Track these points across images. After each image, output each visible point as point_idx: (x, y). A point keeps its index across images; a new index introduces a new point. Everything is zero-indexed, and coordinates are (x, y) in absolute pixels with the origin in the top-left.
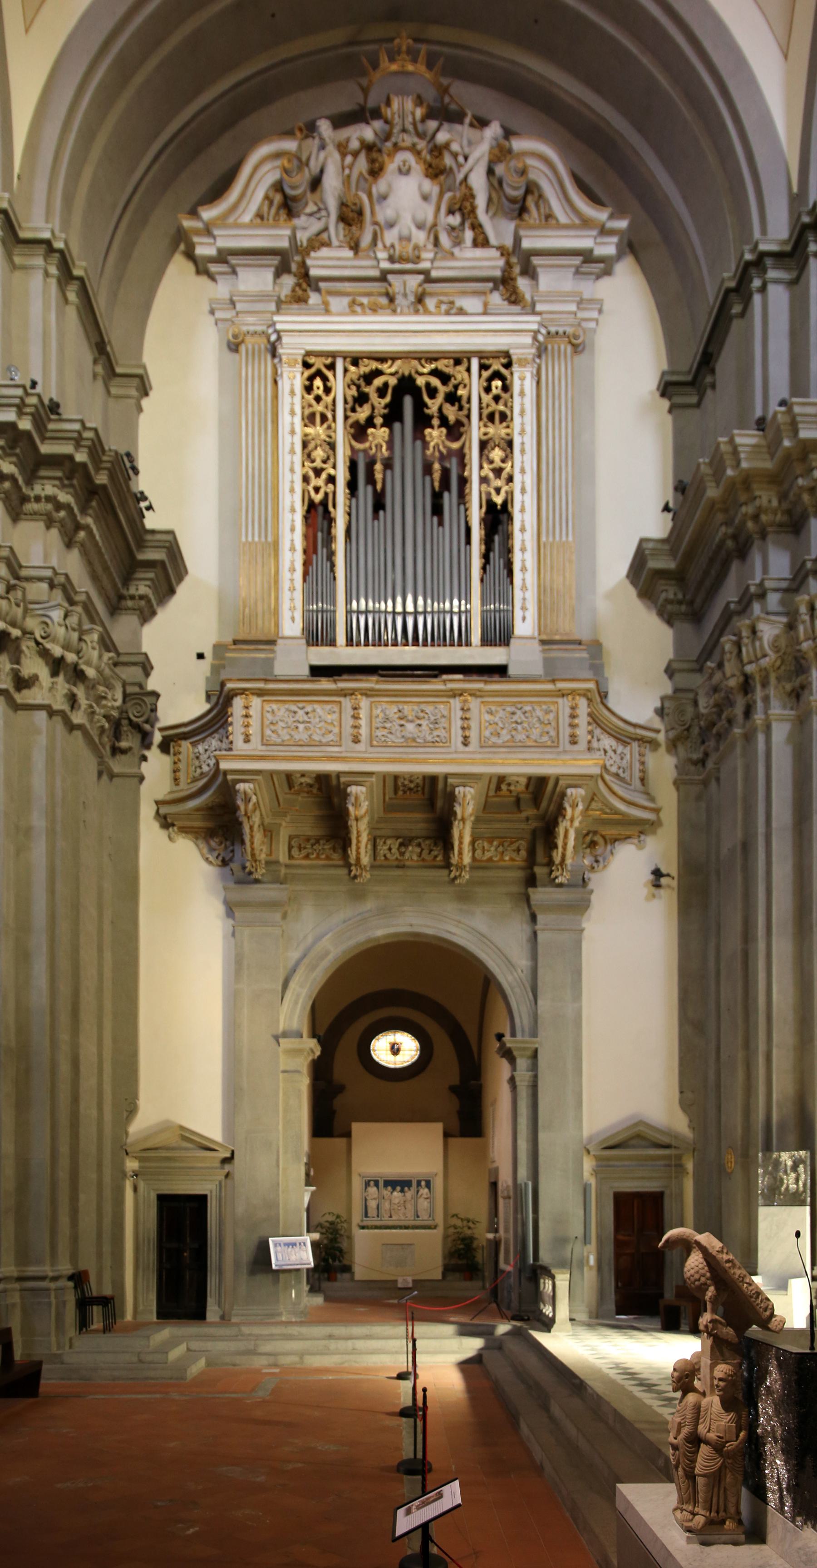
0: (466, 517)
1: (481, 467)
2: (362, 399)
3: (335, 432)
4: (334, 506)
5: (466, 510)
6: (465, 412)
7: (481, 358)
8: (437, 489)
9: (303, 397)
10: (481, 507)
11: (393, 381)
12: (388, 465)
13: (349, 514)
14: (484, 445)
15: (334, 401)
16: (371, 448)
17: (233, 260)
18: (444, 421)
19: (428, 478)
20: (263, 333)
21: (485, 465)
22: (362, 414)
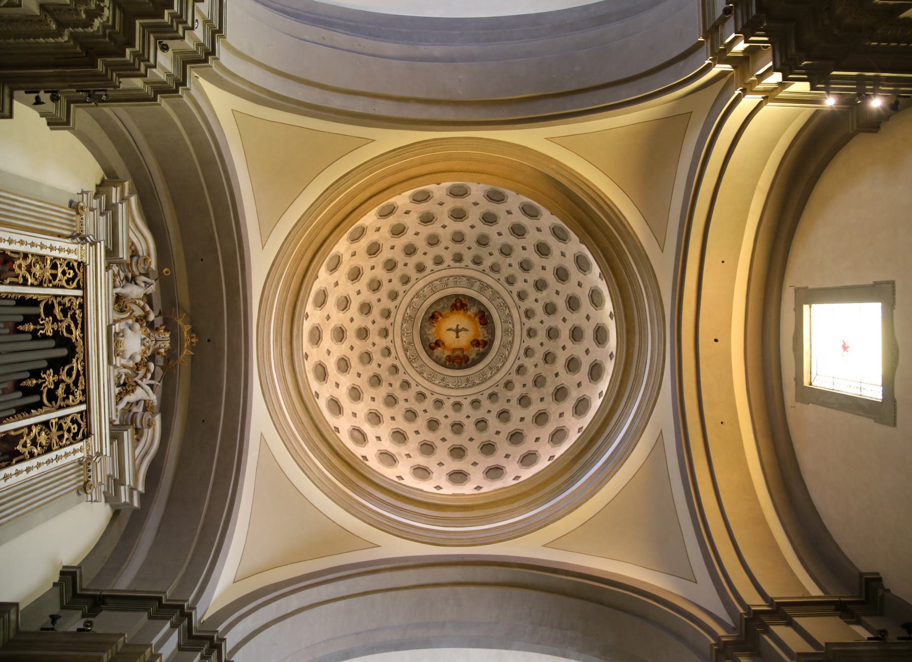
0: (8, 417)
1: (36, 425)
2: (65, 311)
3: (48, 287)
4: (11, 284)
5: (13, 416)
6: (62, 404)
7: (86, 411)
8: (24, 384)
9: (65, 260)
10: (15, 430)
11: (73, 337)
12: (35, 335)
13: (6, 298)
14: (46, 424)
15: (62, 287)
16: (42, 320)
17: (110, 213)
18: (57, 384)
19: (28, 375)
20: (82, 231)
21: (39, 427)
22: (57, 310)
